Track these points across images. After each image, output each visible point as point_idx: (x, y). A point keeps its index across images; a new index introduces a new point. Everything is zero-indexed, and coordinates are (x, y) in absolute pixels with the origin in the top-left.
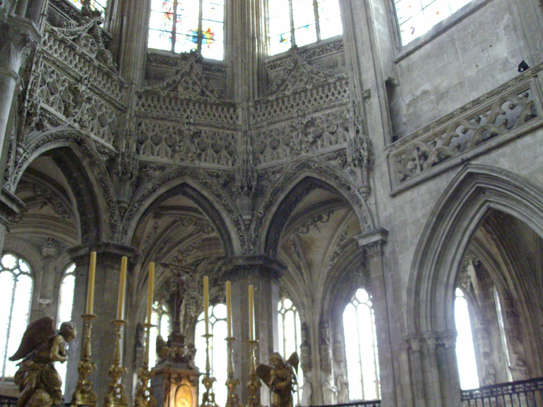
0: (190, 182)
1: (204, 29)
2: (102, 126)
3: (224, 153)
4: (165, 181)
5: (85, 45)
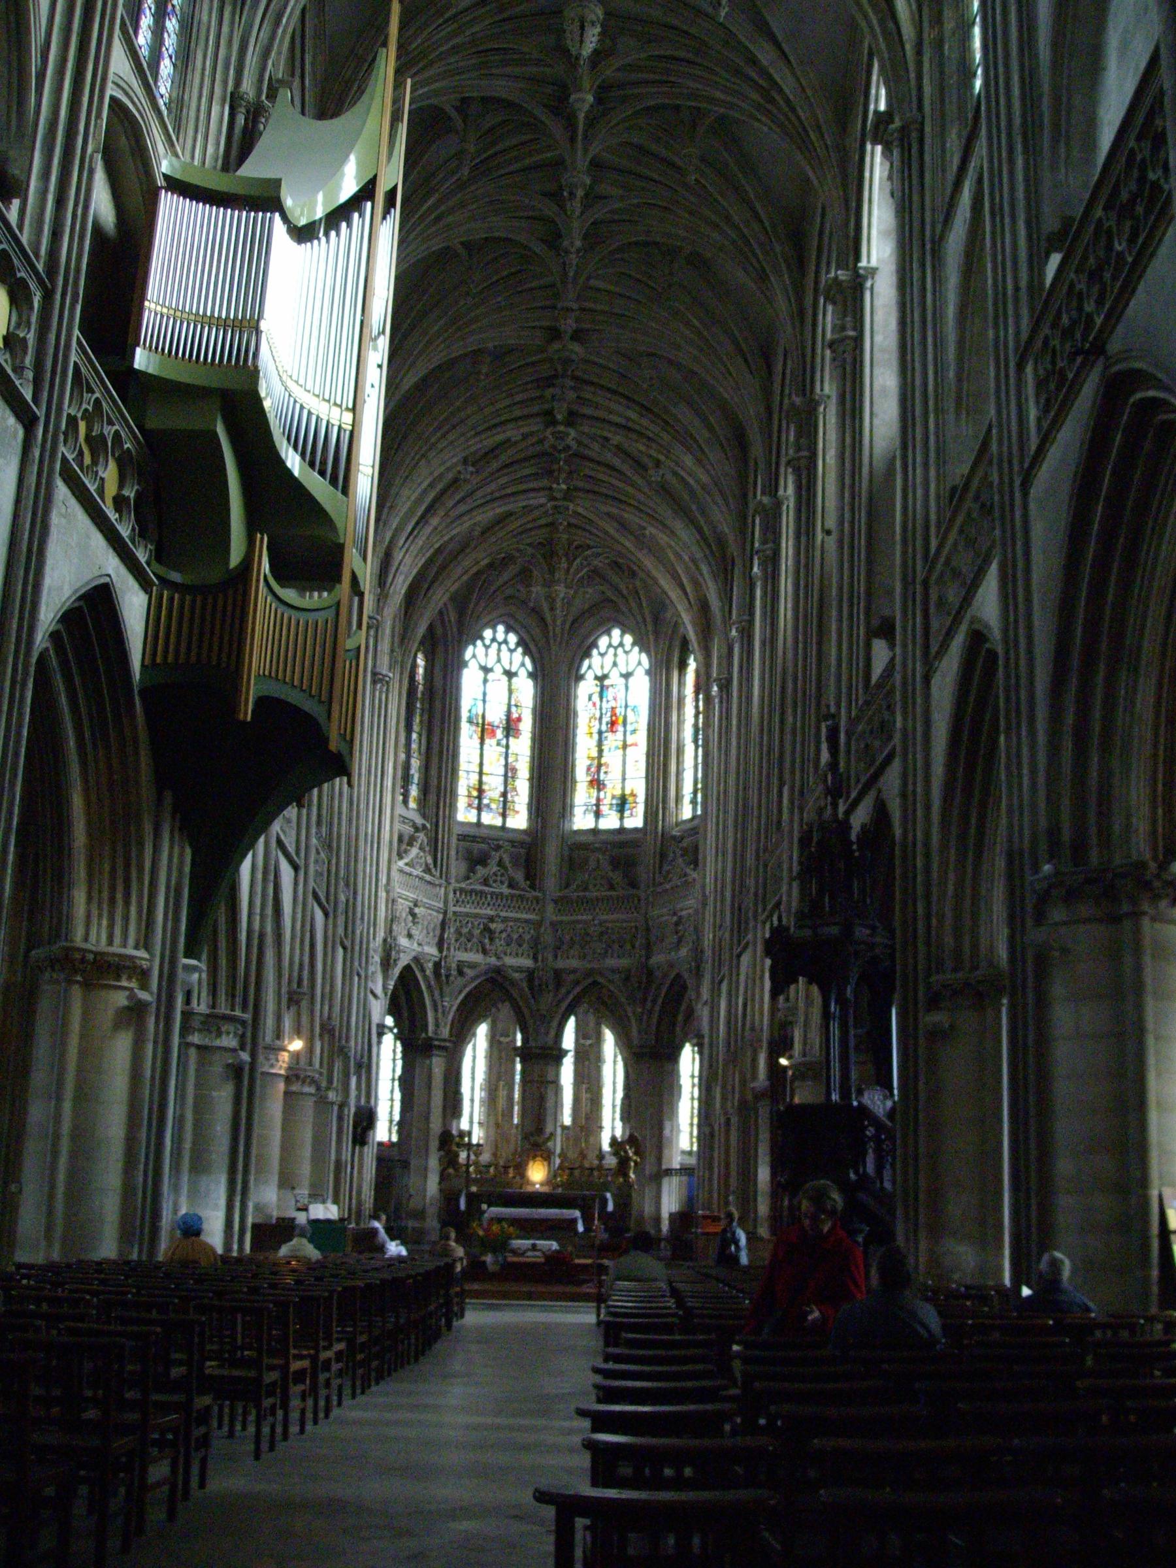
0: (601, 980)
1: (627, 792)
2: (520, 946)
3: (628, 946)
4: (577, 983)
5: (495, 881)
